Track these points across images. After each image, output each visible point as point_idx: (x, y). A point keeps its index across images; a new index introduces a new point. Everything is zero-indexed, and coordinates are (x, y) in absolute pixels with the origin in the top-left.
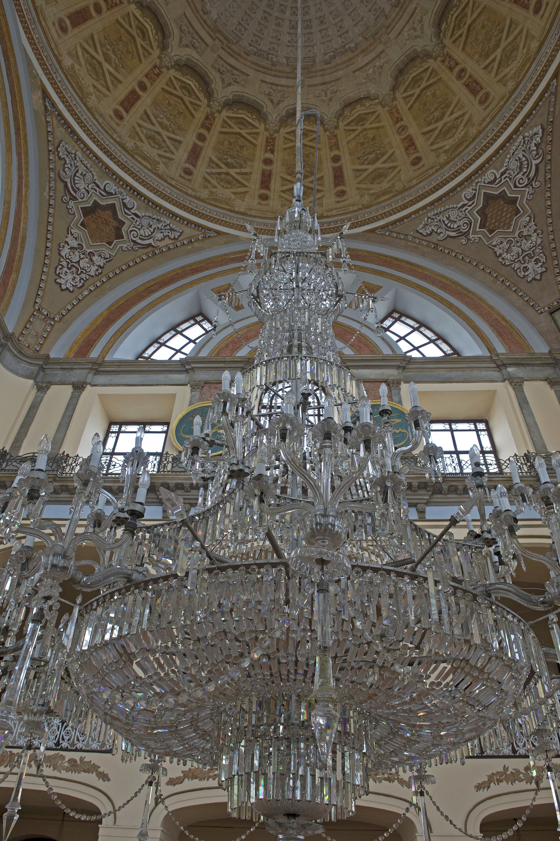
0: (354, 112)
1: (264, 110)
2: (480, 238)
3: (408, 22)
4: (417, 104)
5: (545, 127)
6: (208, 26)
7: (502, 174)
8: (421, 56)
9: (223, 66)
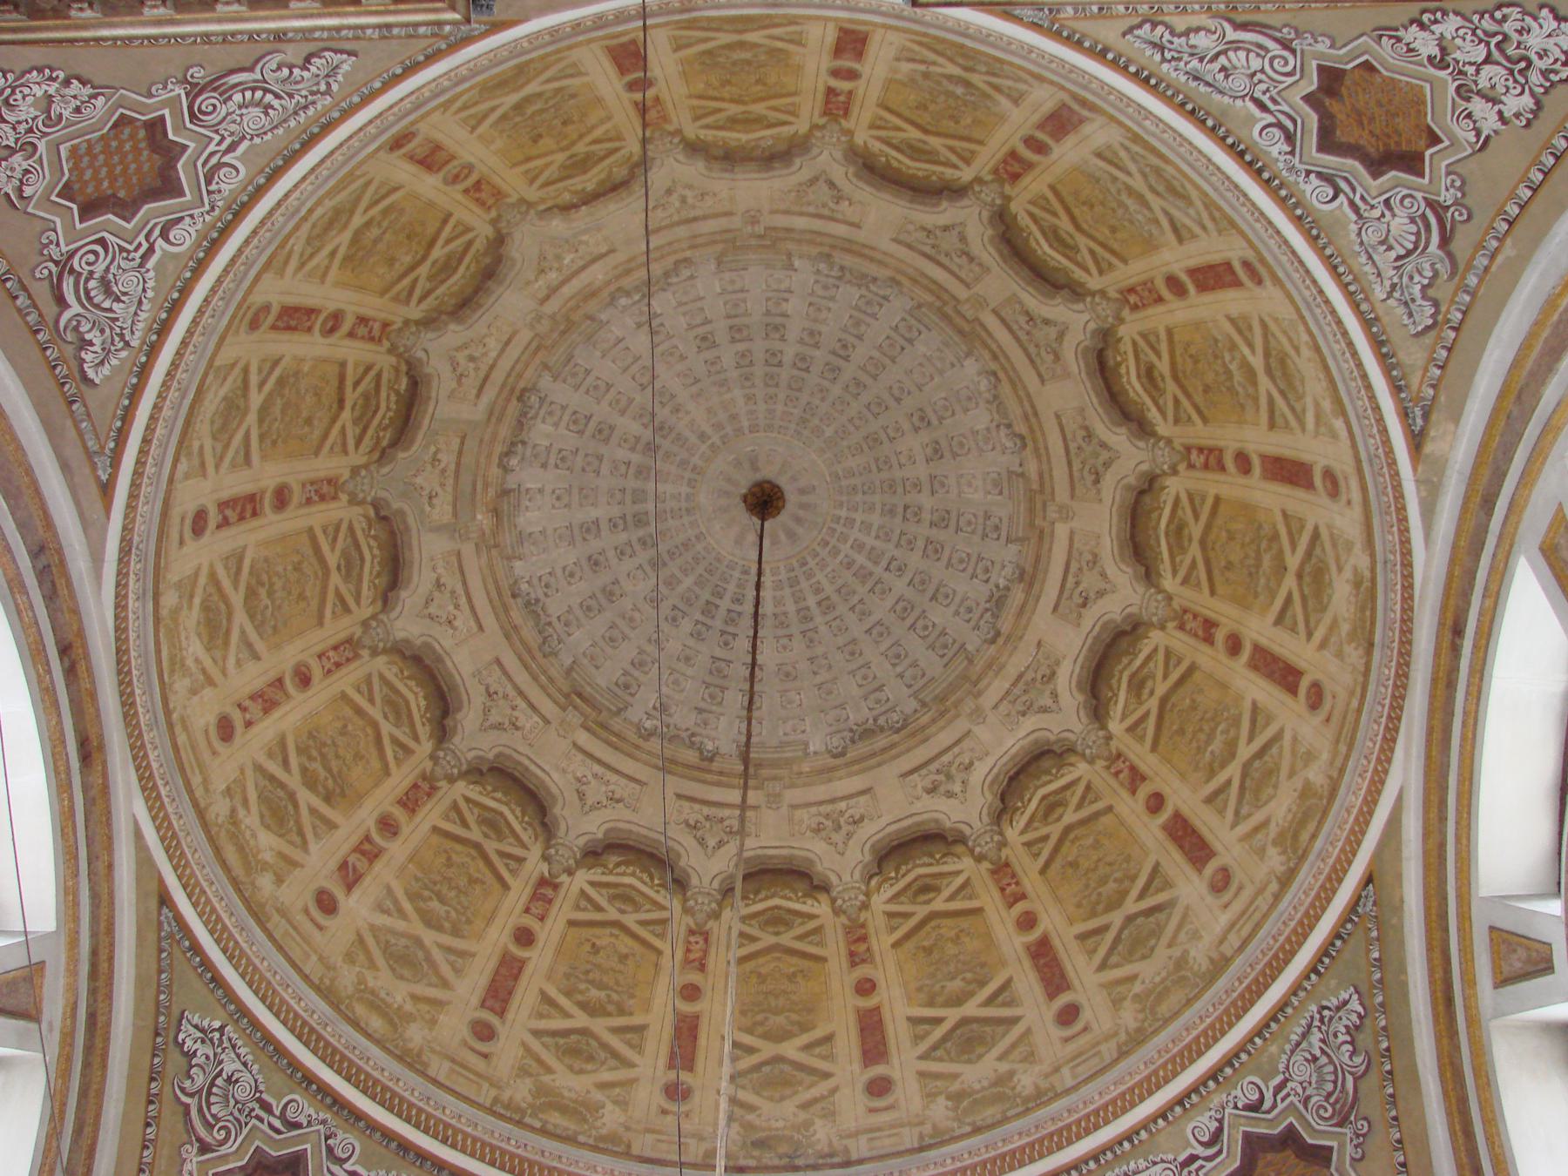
0: (603, 176)
1: (851, 170)
2: (150, 95)
3: (492, 367)
4: (431, 230)
5: (83, 387)
6: (986, 346)
7: (151, 250)
8: (444, 317)
9: (960, 267)
